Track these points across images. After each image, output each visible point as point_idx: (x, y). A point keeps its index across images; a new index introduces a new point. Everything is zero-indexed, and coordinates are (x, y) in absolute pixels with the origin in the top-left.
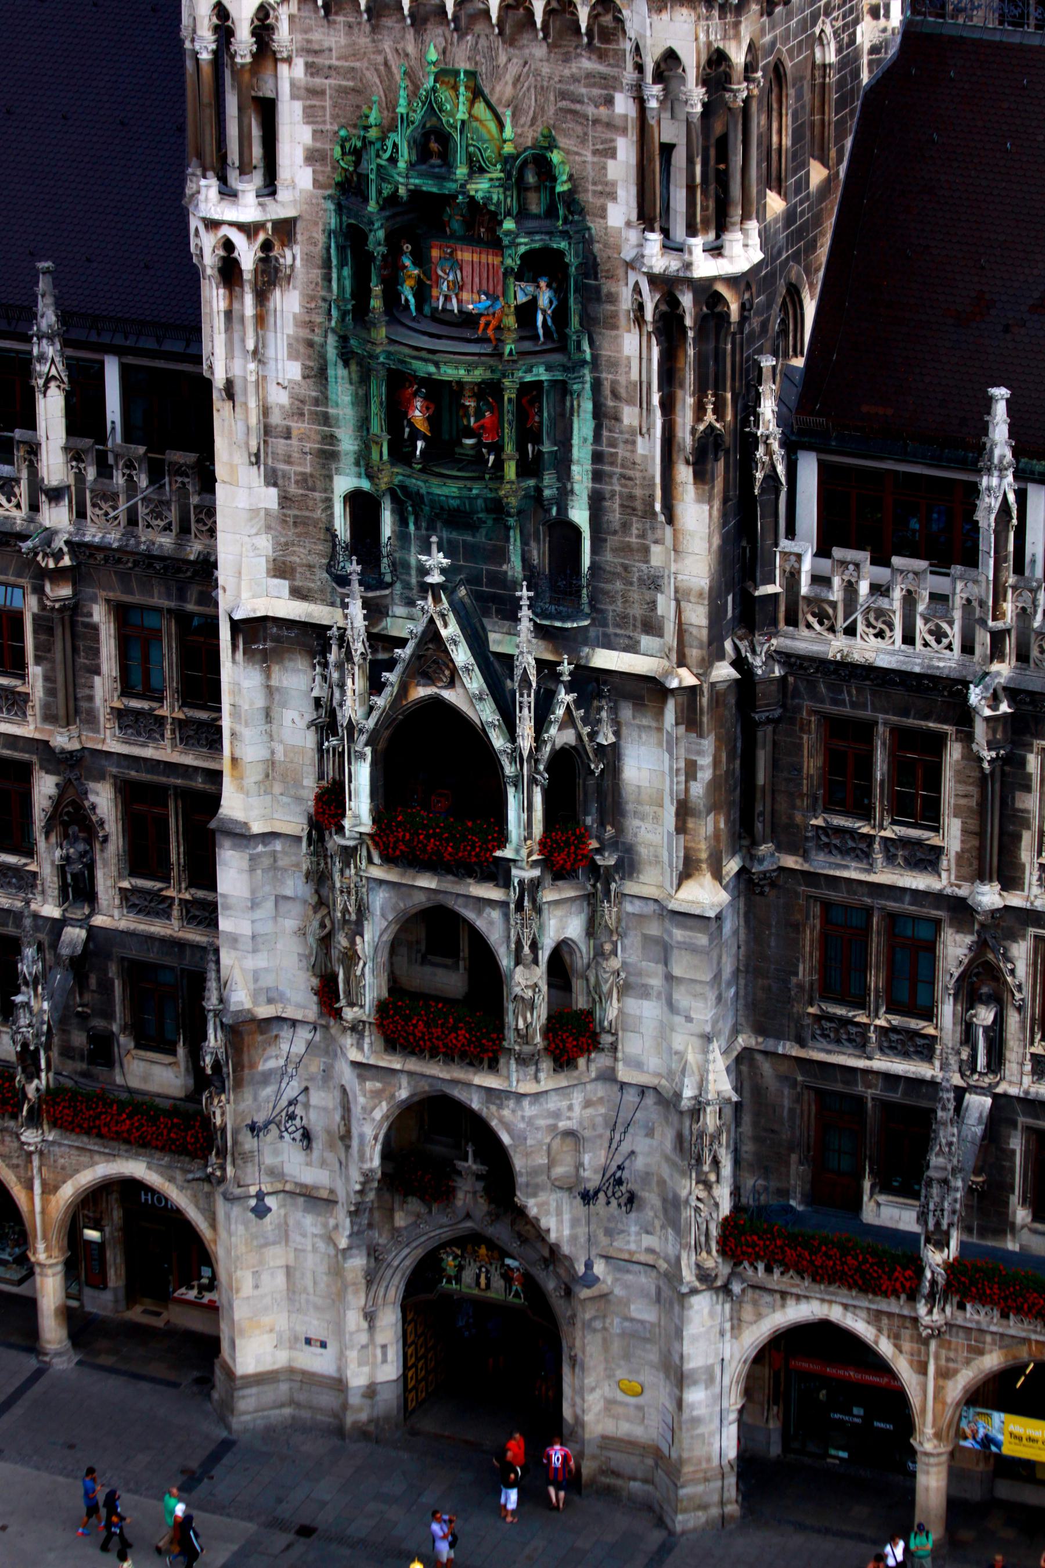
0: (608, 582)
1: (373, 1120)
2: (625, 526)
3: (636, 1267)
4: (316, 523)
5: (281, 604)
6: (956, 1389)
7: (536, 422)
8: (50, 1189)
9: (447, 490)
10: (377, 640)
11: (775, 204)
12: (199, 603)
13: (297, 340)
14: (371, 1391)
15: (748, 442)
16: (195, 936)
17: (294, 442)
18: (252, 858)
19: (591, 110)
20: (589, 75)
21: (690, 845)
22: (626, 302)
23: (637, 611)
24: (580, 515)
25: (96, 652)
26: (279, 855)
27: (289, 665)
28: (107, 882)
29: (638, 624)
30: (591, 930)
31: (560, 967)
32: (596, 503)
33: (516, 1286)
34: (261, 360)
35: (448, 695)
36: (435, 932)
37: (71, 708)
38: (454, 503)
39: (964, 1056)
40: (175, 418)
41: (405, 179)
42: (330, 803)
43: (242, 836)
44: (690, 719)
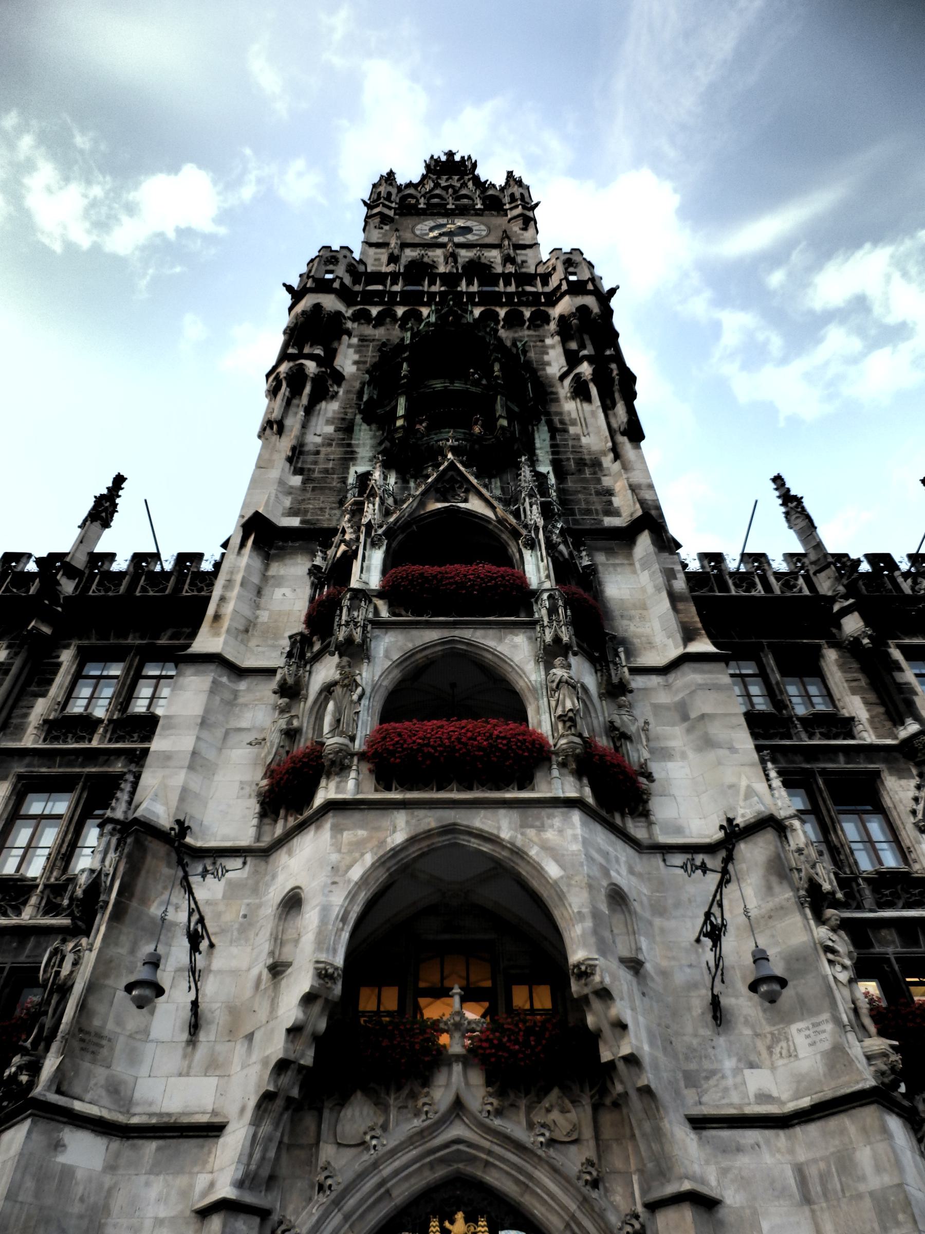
0: (571, 495)
1: (349, 881)
2: (580, 471)
3: (751, 1136)
4: (330, 489)
12: (170, 638)
13: (334, 418)
17: (322, 456)
18: (214, 682)
20: (528, 336)
21: (686, 619)
22: (564, 389)
24: (545, 468)
25: (52, 680)
26: (241, 694)
27: (288, 561)
29: (600, 512)
35: (462, 505)
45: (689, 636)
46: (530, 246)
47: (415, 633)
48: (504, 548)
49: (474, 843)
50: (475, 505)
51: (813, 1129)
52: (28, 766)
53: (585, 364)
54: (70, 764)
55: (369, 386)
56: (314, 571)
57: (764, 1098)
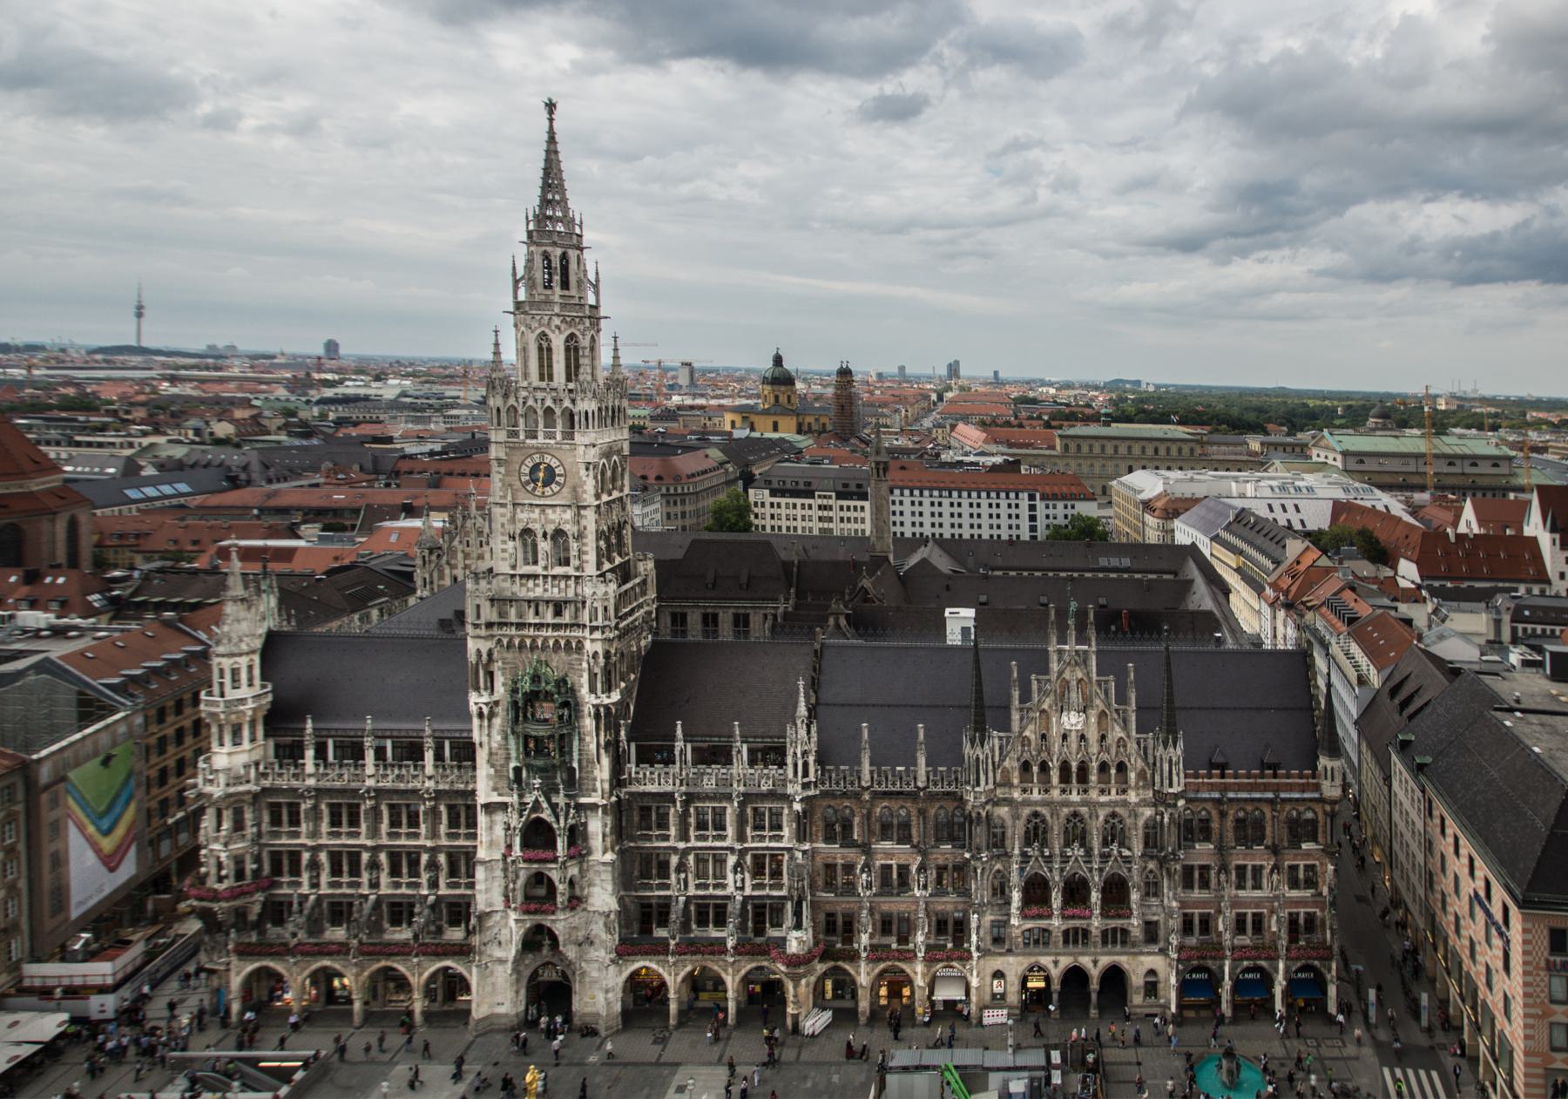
5: (495, 798)
6: (679, 979)
7: (564, 744)
8: (420, 975)
9: (540, 763)
10: (523, 804)
11: (623, 685)
14: (517, 1015)
15: (617, 741)
16: (469, 892)
24: (575, 765)
28: (442, 882)
30: (581, 871)
31: (572, 883)
32: (580, 761)
34: (490, 737)
36: (539, 879)
37: (434, 834)
40: (465, 752)
41: (526, 686)
42: (509, 847)
43: (483, 863)
44: (605, 812)
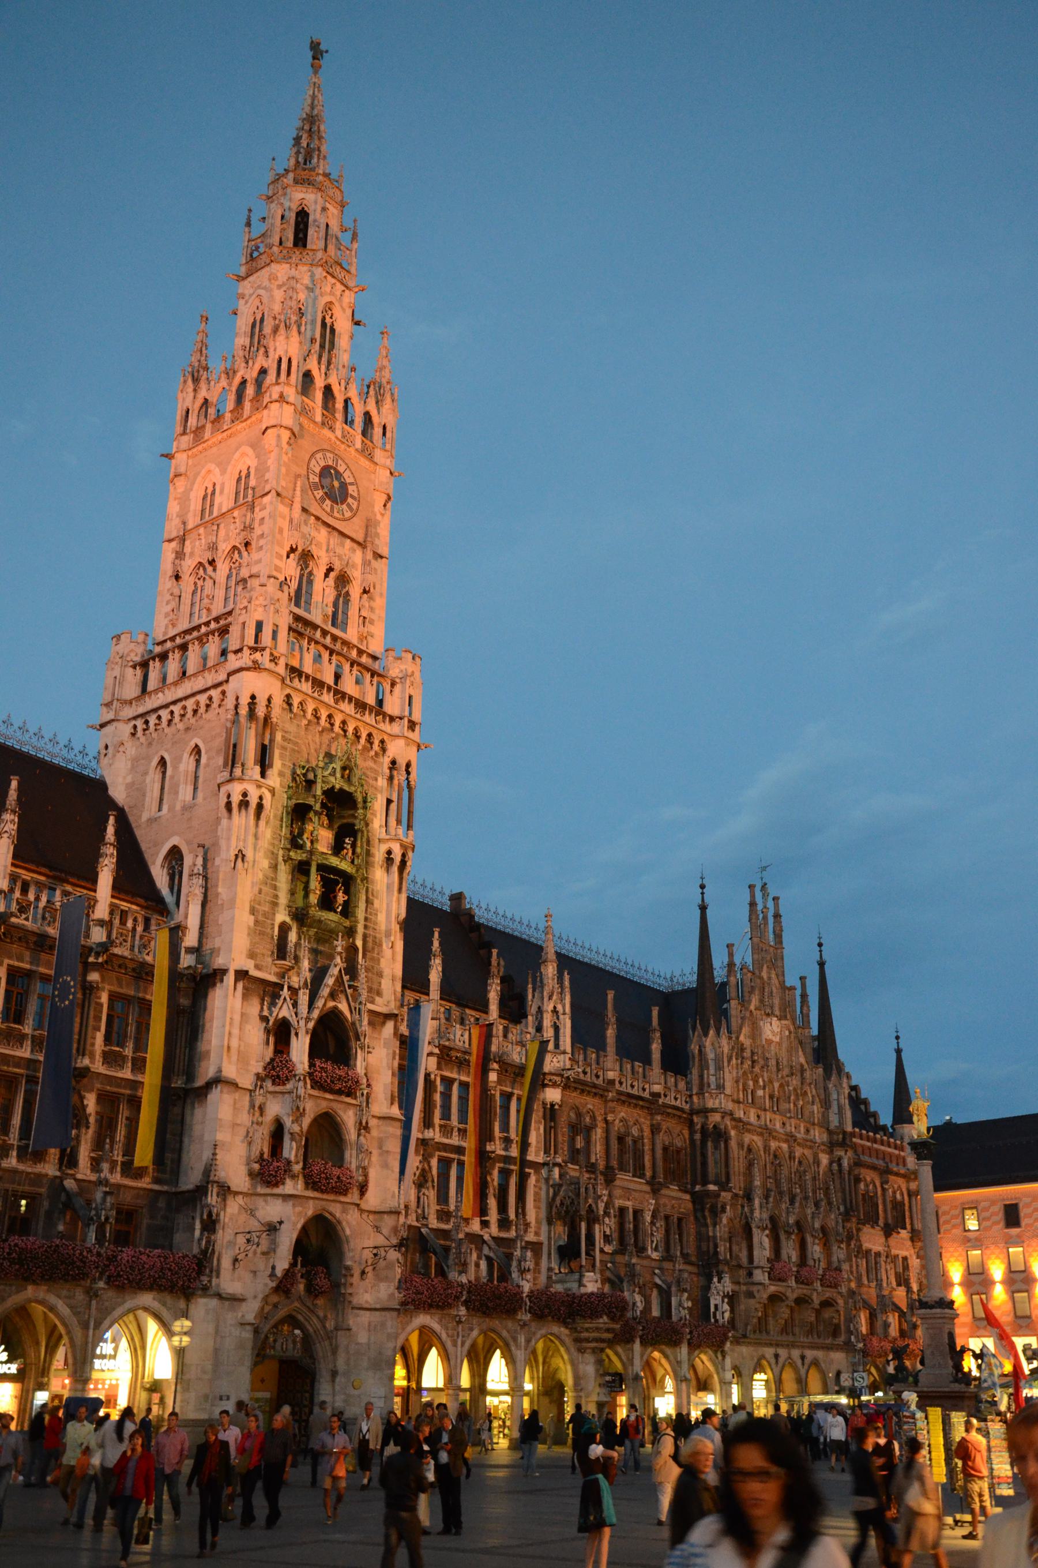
2: (373, 949)
3: (362, 1312)
17: (262, 895)
19: (371, 782)
23: (375, 986)
24: (359, 943)
32: (365, 937)
33: (299, 1345)
35: (340, 1006)
38: (333, 925)
39: (420, 1211)
43: (234, 1085)
45: (392, 1104)
46: (381, 557)
47: (319, 1101)
48: (348, 1039)
49: (327, 1215)
50: (343, 1007)
51: (377, 1313)
52: (102, 1083)
53: (398, 845)
54: (119, 1086)
55: (288, 813)
56: (264, 1019)
57: (367, 1302)
